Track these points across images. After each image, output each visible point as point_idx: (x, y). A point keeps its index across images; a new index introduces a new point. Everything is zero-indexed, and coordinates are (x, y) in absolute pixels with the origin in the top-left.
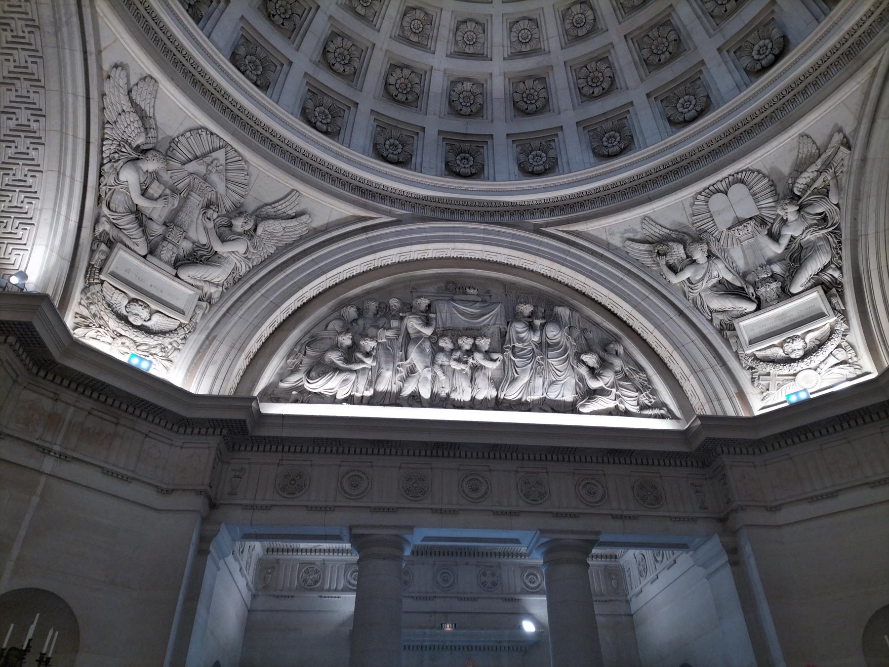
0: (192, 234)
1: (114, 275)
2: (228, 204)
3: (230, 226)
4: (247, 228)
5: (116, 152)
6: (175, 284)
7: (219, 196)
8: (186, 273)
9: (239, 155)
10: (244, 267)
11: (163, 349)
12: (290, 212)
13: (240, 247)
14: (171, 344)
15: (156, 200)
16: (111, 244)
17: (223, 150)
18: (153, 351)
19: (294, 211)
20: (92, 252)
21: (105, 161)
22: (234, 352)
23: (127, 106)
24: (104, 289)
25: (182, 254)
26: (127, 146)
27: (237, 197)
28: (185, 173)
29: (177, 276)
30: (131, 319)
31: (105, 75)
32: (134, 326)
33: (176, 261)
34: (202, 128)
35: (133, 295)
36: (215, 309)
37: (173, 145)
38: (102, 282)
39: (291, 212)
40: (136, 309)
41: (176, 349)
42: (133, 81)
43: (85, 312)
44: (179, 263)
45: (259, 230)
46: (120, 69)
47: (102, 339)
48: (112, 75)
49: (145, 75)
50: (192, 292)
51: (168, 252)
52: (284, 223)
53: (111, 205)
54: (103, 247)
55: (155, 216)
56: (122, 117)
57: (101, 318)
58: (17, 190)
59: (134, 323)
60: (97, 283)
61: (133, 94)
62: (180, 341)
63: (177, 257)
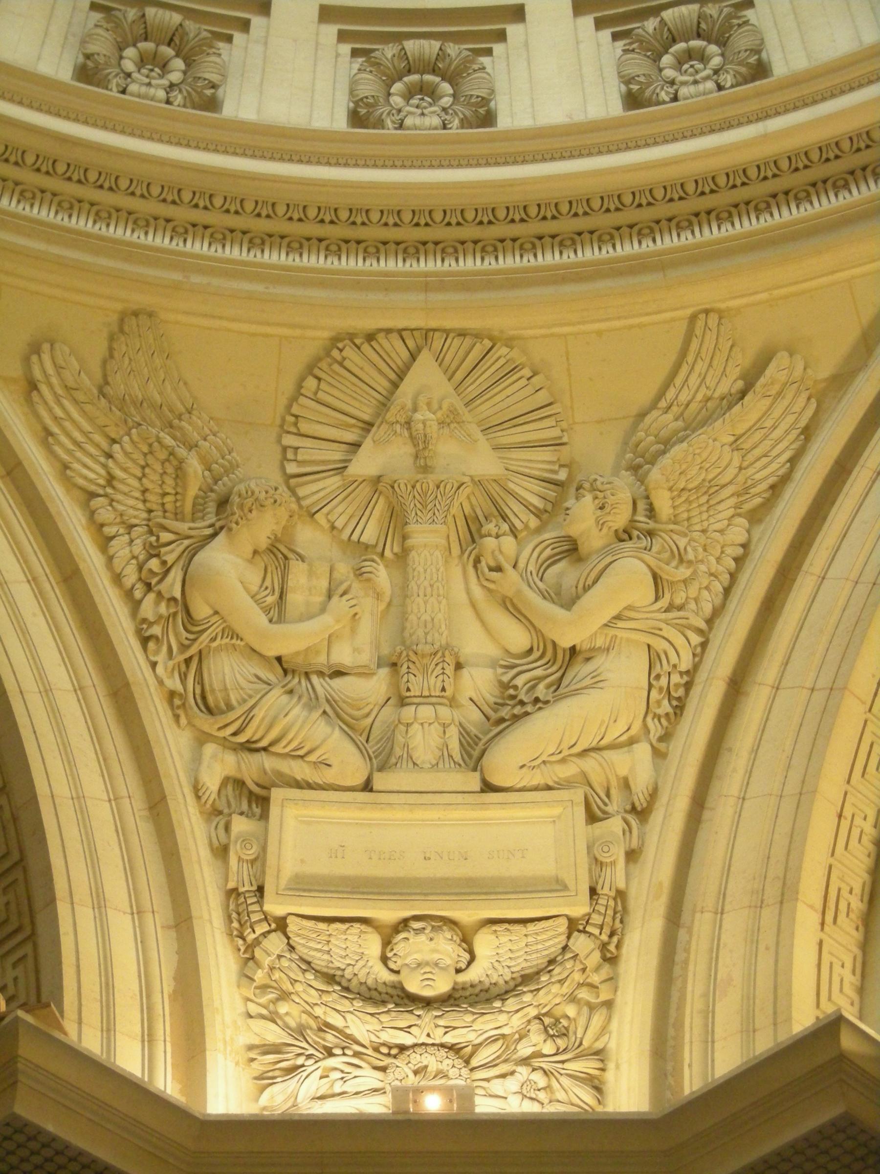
1: (304, 885)
2: (532, 493)
3: (571, 550)
4: (620, 519)
7: (494, 489)
8: (509, 758)
9: (478, 336)
10: (679, 641)
11: (553, 1026)
12: (724, 388)
13: (627, 581)
14: (572, 999)
15: (323, 610)
16: (258, 801)
17: (425, 358)
18: (524, 1050)
19: (734, 372)
20: (221, 852)
21: (138, 594)
22: (768, 916)
24: (295, 940)
27: (546, 455)
28: (365, 491)
29: (488, 787)
30: (413, 986)
32: (428, 1003)
35: (388, 913)
36: (657, 818)
37: (290, 440)
38: (281, 925)
39: (730, 384)
40: (413, 948)
41: (592, 1008)
43: (273, 1034)
44: (473, 753)
45: (663, 503)
46: (46, 347)
47: (350, 1087)
49: (115, 317)
50: (557, 811)
51: (427, 735)
52: (722, 431)
53: (210, 700)
54: (241, 825)
55: (343, 655)
57: (325, 1027)
59: (427, 993)
60: (265, 935)
62: (595, 979)
63: (464, 732)
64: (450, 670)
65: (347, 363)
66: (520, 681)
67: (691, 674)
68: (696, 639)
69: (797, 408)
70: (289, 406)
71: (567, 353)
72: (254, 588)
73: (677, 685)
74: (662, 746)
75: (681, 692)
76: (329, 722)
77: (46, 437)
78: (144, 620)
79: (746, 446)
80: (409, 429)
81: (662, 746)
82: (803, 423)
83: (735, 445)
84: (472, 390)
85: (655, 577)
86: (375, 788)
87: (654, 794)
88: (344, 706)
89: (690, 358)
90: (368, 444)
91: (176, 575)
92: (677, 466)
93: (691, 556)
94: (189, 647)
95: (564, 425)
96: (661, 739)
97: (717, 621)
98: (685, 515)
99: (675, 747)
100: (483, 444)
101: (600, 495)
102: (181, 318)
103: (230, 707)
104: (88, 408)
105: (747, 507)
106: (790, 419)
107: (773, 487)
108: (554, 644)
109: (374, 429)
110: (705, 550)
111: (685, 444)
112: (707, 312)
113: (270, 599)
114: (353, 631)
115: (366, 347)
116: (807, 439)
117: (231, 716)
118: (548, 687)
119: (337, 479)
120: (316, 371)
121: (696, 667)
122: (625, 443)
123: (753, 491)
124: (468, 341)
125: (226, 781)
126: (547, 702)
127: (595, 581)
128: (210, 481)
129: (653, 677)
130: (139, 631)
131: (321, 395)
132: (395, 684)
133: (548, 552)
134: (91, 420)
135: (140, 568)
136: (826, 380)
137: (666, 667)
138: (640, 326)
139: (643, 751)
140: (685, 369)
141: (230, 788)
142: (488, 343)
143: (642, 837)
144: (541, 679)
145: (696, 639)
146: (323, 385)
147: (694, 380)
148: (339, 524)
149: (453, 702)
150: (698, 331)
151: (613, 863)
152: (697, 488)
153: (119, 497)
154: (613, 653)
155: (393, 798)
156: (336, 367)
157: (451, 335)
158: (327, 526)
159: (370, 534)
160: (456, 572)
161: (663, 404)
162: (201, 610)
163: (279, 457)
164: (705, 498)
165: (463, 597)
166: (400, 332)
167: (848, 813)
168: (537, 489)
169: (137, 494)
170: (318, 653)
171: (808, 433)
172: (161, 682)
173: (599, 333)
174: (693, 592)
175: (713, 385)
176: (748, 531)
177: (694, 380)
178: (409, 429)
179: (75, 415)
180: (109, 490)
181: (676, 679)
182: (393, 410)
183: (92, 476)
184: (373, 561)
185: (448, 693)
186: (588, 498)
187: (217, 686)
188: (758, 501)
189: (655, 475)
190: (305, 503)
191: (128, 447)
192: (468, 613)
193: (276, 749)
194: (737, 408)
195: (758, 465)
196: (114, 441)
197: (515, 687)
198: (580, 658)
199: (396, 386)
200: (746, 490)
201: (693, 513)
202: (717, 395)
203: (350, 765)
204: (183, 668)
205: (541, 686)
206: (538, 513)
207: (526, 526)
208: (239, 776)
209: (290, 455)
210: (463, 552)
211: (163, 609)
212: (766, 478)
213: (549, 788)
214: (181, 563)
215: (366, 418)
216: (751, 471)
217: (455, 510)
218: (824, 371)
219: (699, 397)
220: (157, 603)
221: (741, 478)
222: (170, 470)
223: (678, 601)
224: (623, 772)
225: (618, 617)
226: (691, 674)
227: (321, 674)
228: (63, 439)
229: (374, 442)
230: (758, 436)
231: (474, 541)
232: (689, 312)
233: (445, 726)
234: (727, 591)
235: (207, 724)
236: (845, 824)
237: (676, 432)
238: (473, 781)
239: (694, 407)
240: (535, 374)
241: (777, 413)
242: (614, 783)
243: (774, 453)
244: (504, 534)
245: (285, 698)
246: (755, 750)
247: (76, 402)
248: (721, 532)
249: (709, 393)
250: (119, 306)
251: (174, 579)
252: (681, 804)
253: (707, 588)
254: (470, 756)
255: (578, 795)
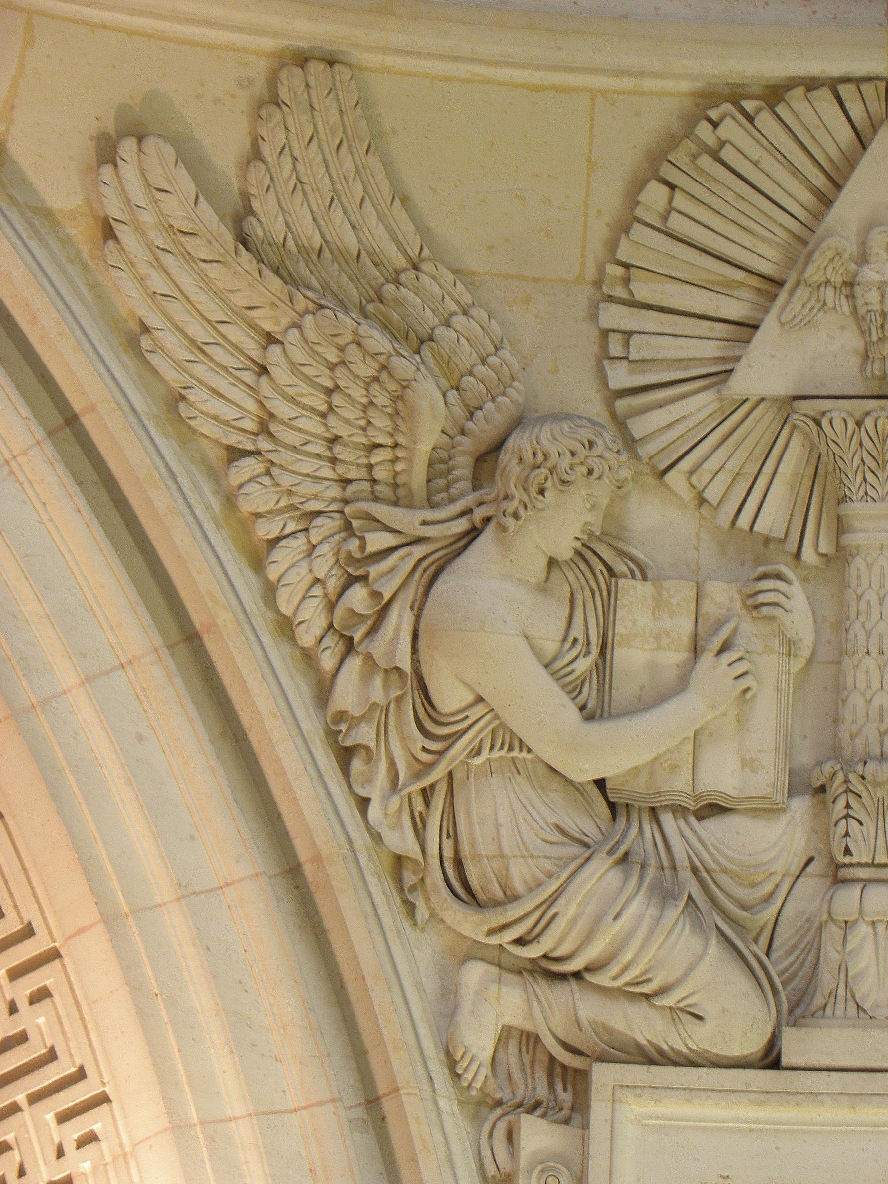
5: (351, 581)
15: (683, 682)
21: (328, 662)
23: (263, 298)
26: (382, 511)
28: (762, 422)
31: (80, 232)
34: (714, 100)
37: (615, 317)
42: (224, 144)
46: (128, 147)
48: (114, 210)
49: (259, 69)
54: (538, 1136)
55: (722, 775)
56: (281, 374)
58: (21, 1099)
61: (269, 222)
65: (727, 154)
70: (612, 245)
72: (551, 647)
76: (699, 927)
77: (135, 338)
78: (341, 716)
80: (851, 297)
86: (785, 1061)
88: (724, 879)
90: (770, 326)
91: (400, 620)
94: (430, 766)
102: (390, 60)
103: (512, 897)
104: (214, 271)
109: (783, 296)
113: (583, 665)
114: (742, 721)
115: (765, 120)
117: (513, 912)
119: (708, 397)
120: (668, 172)
125: (506, 1034)
128: (459, 411)
130: (332, 735)
131: (677, 223)
132: (822, 830)
134: (219, 295)
135: (331, 606)
141: (513, 1048)
146: (680, 201)
148: (712, 494)
153: (283, 457)
155: (818, 1081)
156: (705, 161)
158: (688, 496)
159: (772, 519)
162: (450, 696)
163: (595, 349)
166: (834, 84)
169: (318, 448)
170: (674, 768)
172: (377, 838)
178: (851, 297)
179: (188, 283)
180: (264, 444)
182: (820, 259)
183: (230, 413)
184: (779, 577)
187: (486, 848)
190: (646, 450)
191: (299, 355)
193: (603, 979)
196: (270, 339)
199: (827, 202)
203: (736, 1017)
204: (419, 805)
208: (529, 1027)
209: (615, 347)
211: (377, 692)
214: (409, 595)
215: (766, 268)
220: (367, 676)
222: (382, 400)
227: (679, 810)
228: (169, 339)
229: (782, 325)
235: (469, 924)
245: (614, 877)
247: (188, 256)
250: (268, 44)
251: (397, 630)
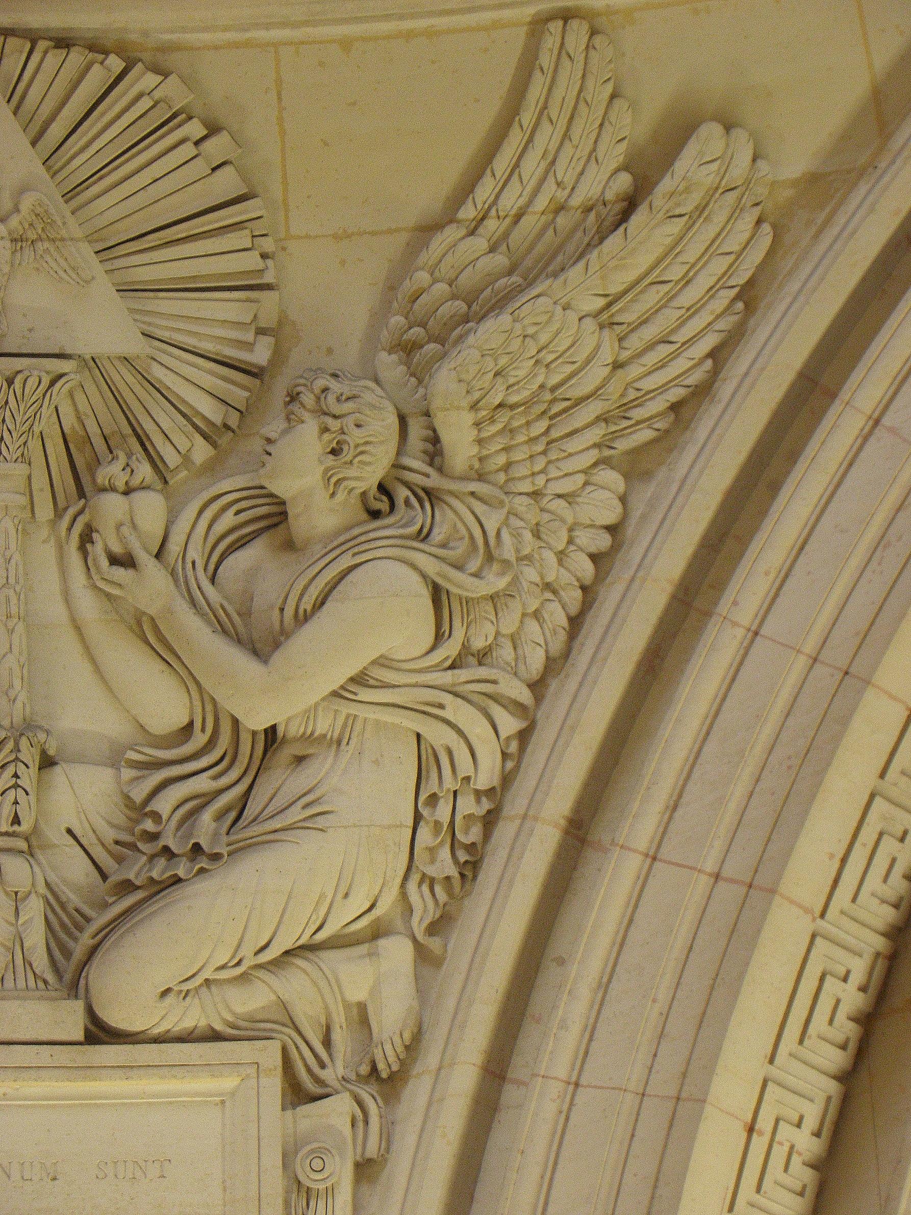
0: (82, 713)
2: (200, 390)
3: (273, 519)
4: (369, 474)
6: (118, 1086)
7: (124, 378)
8: (139, 980)
9: (98, 48)
13: (382, 614)
19: (613, 154)
25: (74, 870)
27: (230, 307)
29: (99, 1033)
33: (64, 923)
36: (417, 1092)
39: (604, 181)
44: (73, 956)
45: (460, 439)
50: (229, 1083)
52: (584, 288)
63: (54, 900)
64: (28, 778)
66: (164, 804)
67: (496, 797)
68: (509, 724)
69: (733, 244)
71: (279, 81)
73: (469, 818)
74: (434, 944)
75: (474, 835)
79: (630, 317)
81: (434, 944)
82: (741, 278)
83: (605, 319)
84: (82, 166)
85: (437, 593)
87: (413, 1047)
89: (527, 117)
92: (490, 363)
93: (508, 551)
95: (268, 245)
96: (433, 929)
97: (554, 685)
98: (501, 460)
99: (461, 943)
100: (103, 287)
101: (334, 425)
105: (623, 445)
106: (719, 266)
107: (675, 407)
108: (236, 722)
110: (537, 535)
111: (505, 319)
112: (566, 16)
116: (750, 309)
118: (219, 817)
121: (507, 780)
122: (392, 287)
123: (637, 414)
124: (77, 57)
126: (215, 857)
127: (320, 604)
129: (424, 802)
133: (228, 520)
136: (795, 183)
137: (450, 783)
138: (430, 33)
139: (398, 952)
140: (516, 138)
142: (116, 63)
143: (387, 1138)
144: (209, 798)
145: (509, 724)
147: (532, 166)
149: (31, 846)
150: (546, 59)
151: (330, 1191)
152: (527, 404)
154: (348, 752)
157: (42, 45)
160: (45, 553)
161: (468, 212)
164: (540, 427)
165: (58, 611)
167: (765, 1123)
168: (208, 381)
171: (749, 297)
173: (346, 44)
174: (509, 624)
175: (569, 180)
176: (623, 499)
177: (532, 166)
181: (468, 805)
185: (25, 827)
186: (310, 427)
188: (645, 435)
189: (445, 383)
192: (68, 642)
194: (614, 241)
195: (651, 359)
197: (156, 817)
198: (285, 754)
200: (626, 407)
201: (518, 456)
202: (576, 201)
205: (207, 817)
206: (209, 433)
207: (186, 459)
210: (59, 513)
212: (663, 388)
213: (215, 1037)
216: (634, 371)
217: (46, 423)
218: (794, 161)
219: (541, 203)
221: (614, 389)
223: (478, 643)
224: (357, 993)
225: (360, 680)
226: (496, 797)
230: (653, 296)
231: (81, 494)
232: (530, 11)
233: (18, 900)
234: (576, 623)
236: (759, 1144)
237: (491, 279)
238: (73, 1023)
239: (529, 223)
240: (213, 129)
241: (692, 253)
242: (339, 1018)
243: (681, 337)
244: (143, 488)
246: (604, 986)
248: (568, 497)
249: (562, 195)
252: (464, 1079)
253: (537, 615)
254: (67, 954)
255: (269, 1054)
